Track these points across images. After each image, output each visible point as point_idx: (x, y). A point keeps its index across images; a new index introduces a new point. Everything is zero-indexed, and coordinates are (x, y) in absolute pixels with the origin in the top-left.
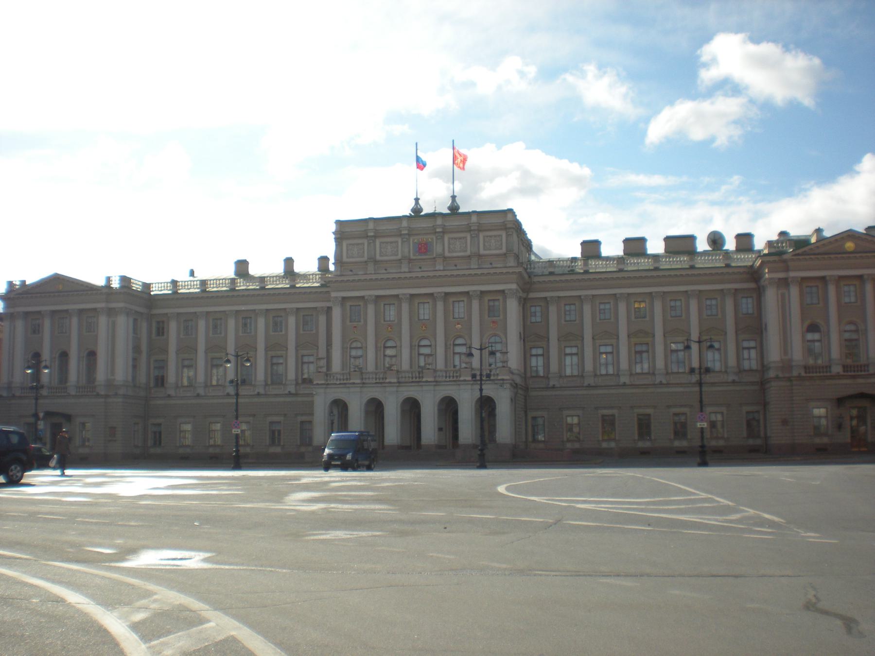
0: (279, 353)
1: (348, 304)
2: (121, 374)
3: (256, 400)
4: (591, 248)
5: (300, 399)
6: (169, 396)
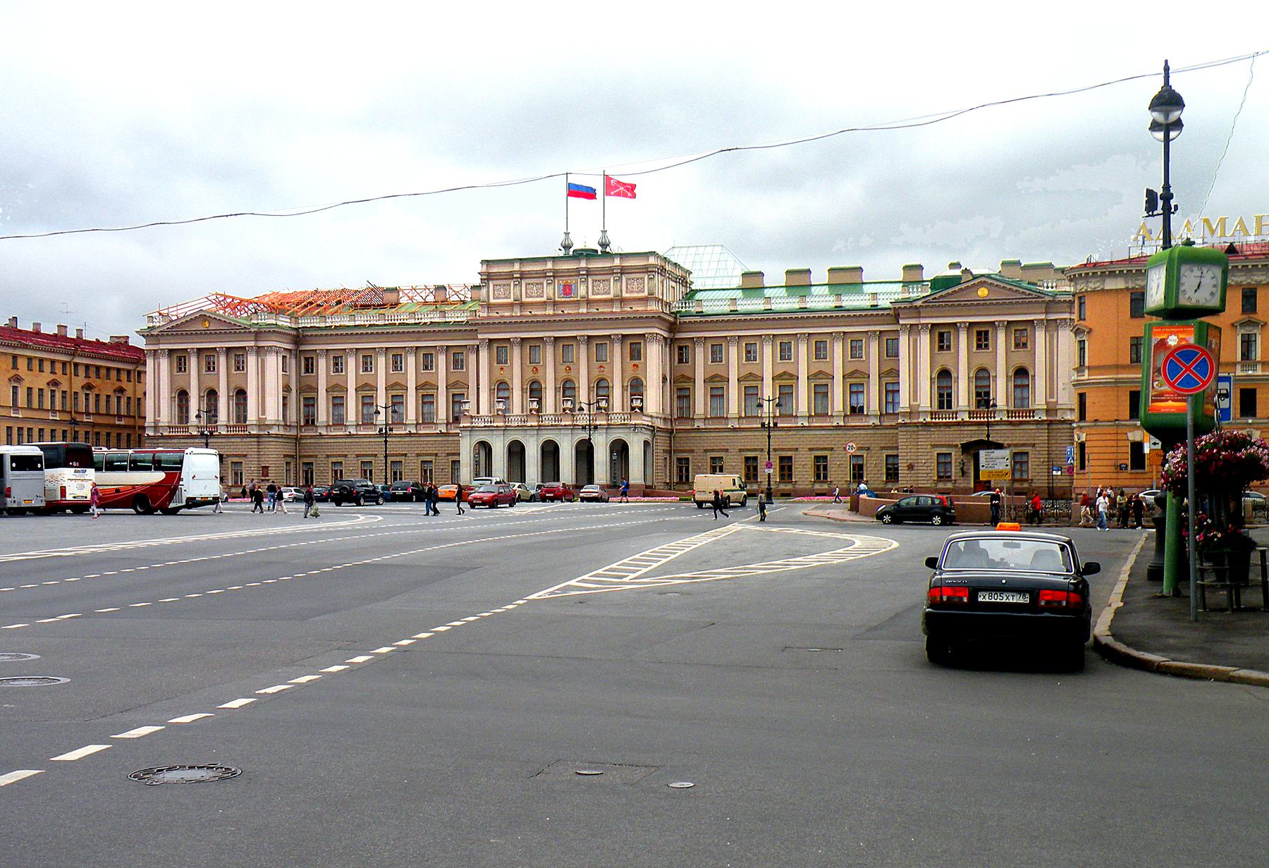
1: (495, 345)
2: (273, 413)
4: (753, 283)
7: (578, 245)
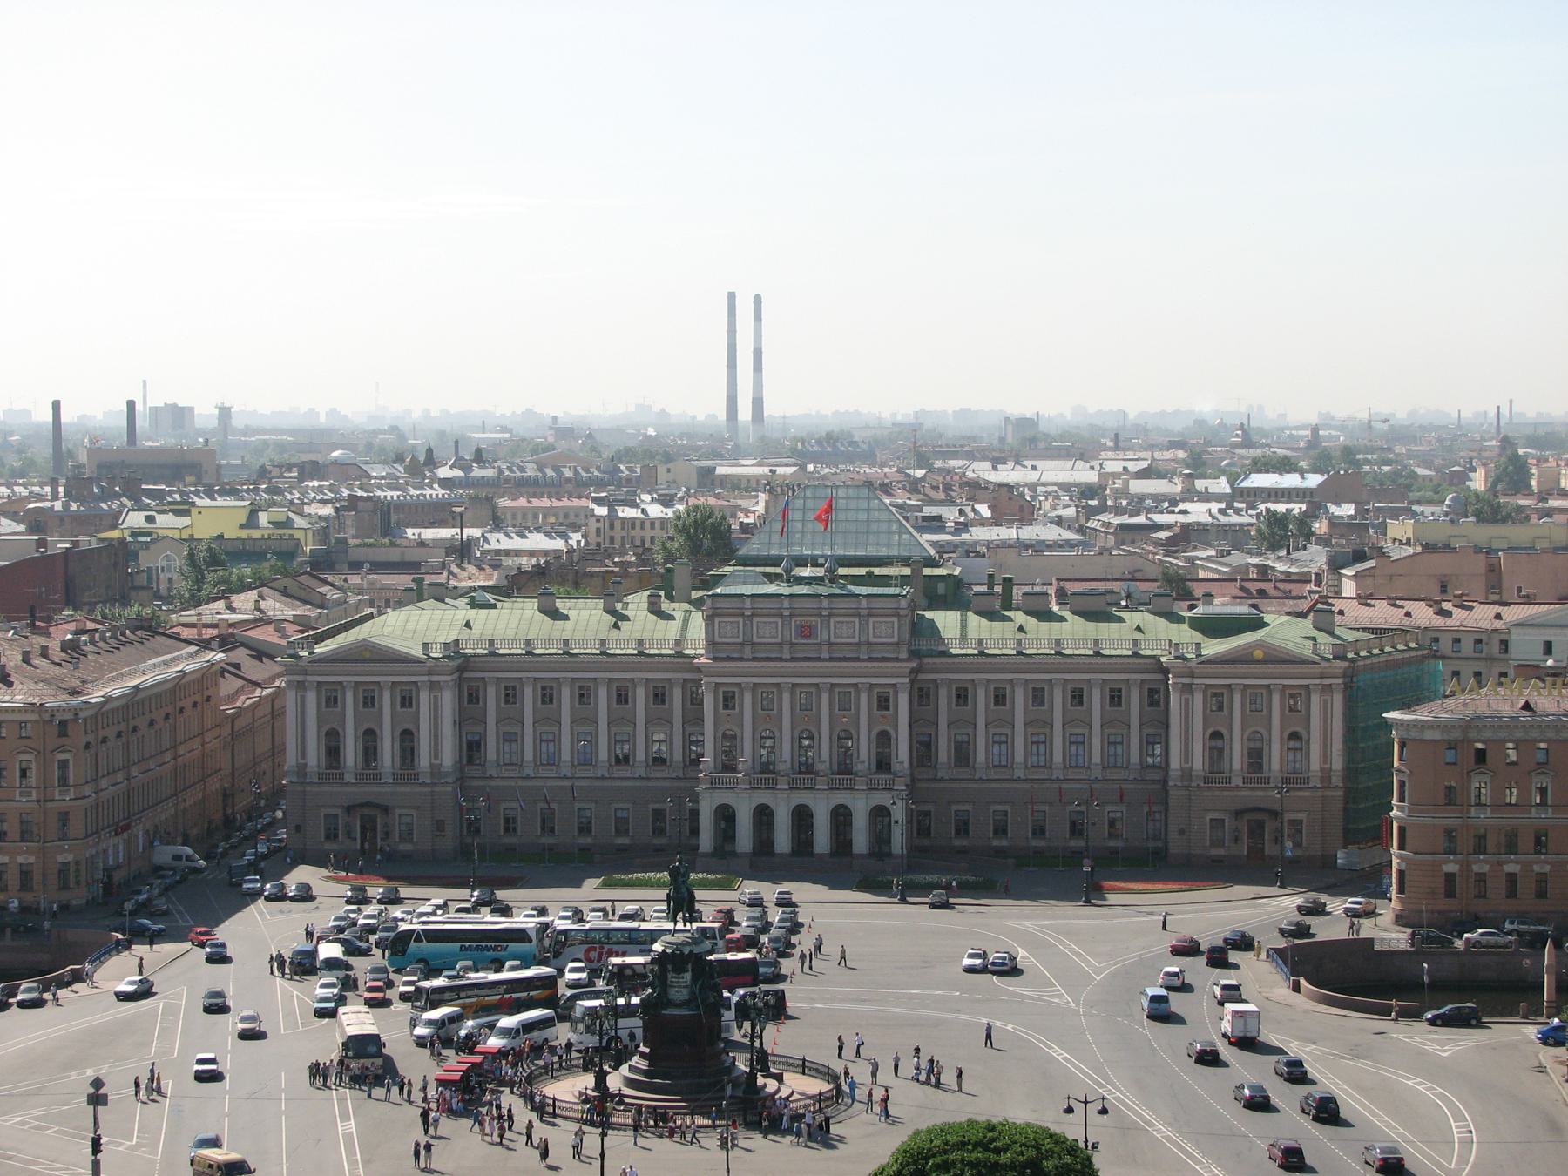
0: (625, 729)
3: (598, 784)
5: (650, 784)
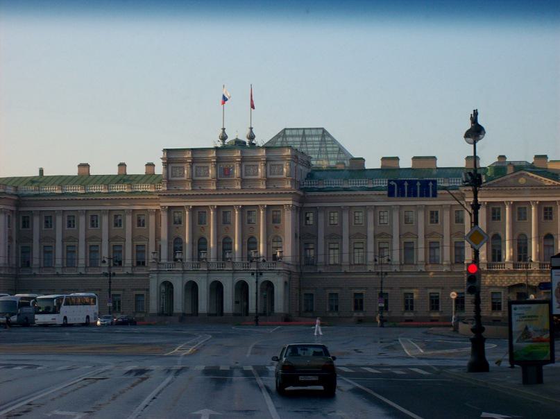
5: (134, 278)
6: (35, 275)
7: (231, 138)
